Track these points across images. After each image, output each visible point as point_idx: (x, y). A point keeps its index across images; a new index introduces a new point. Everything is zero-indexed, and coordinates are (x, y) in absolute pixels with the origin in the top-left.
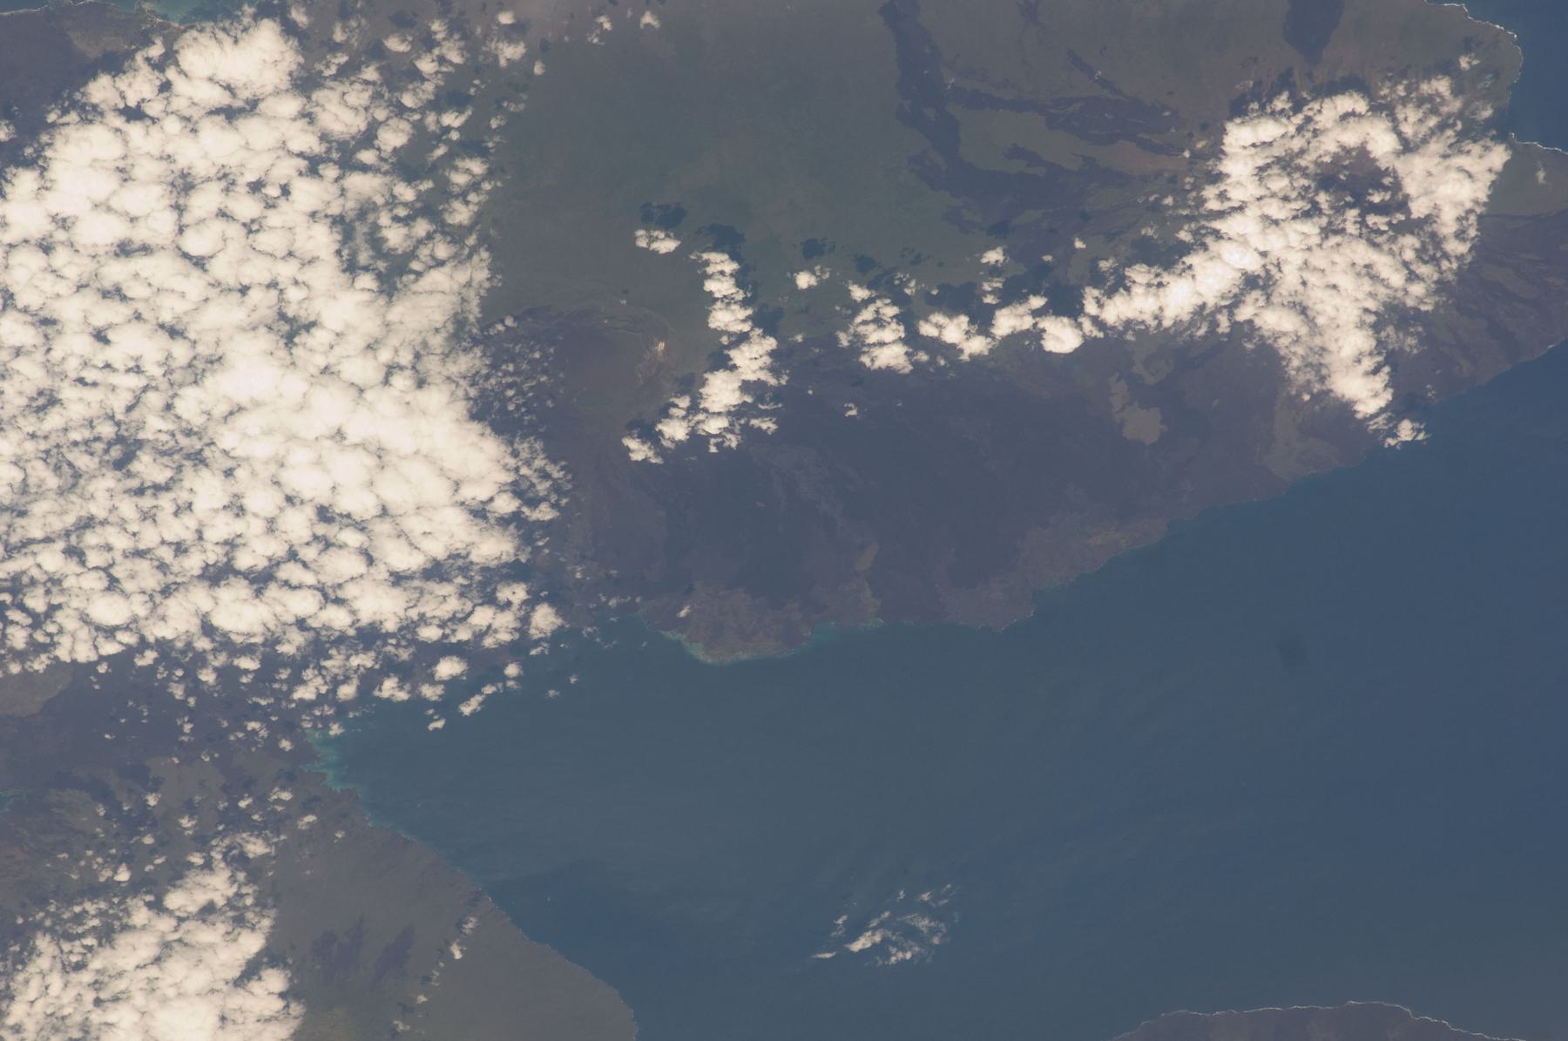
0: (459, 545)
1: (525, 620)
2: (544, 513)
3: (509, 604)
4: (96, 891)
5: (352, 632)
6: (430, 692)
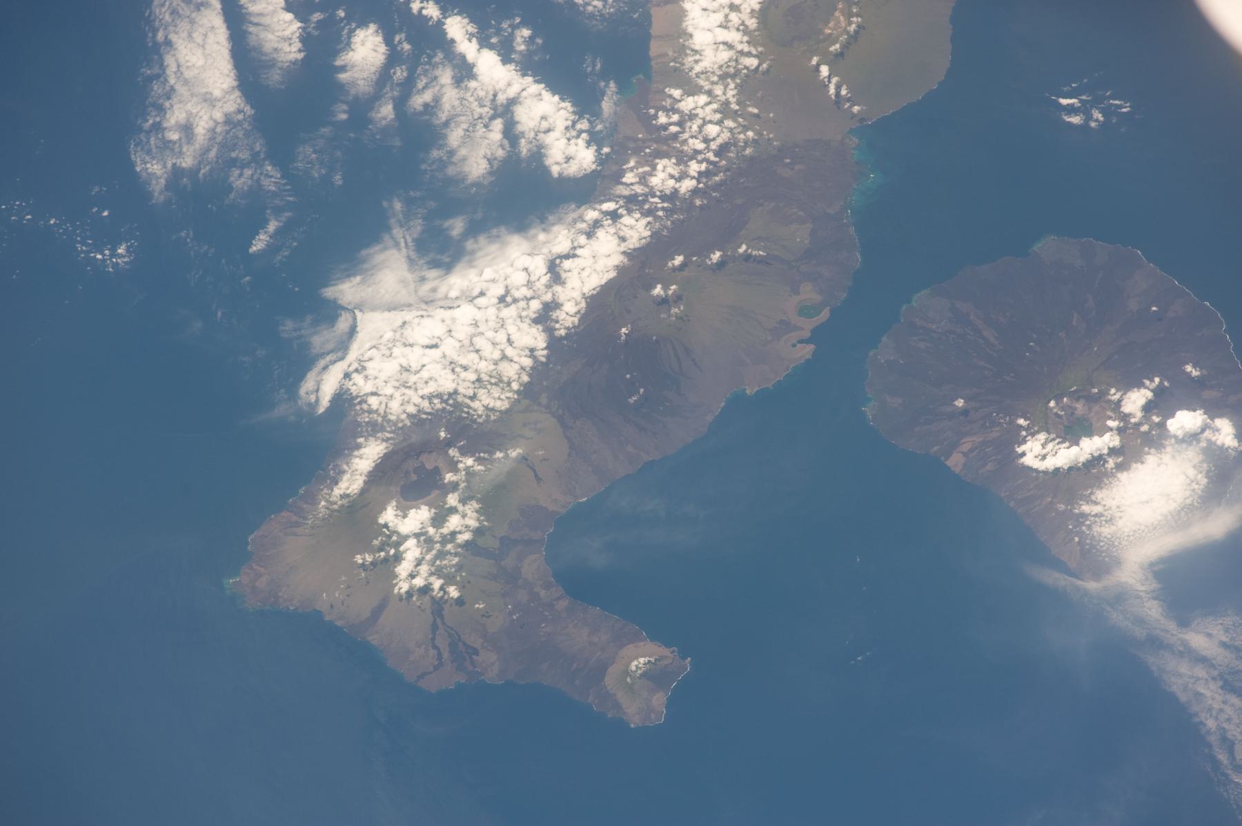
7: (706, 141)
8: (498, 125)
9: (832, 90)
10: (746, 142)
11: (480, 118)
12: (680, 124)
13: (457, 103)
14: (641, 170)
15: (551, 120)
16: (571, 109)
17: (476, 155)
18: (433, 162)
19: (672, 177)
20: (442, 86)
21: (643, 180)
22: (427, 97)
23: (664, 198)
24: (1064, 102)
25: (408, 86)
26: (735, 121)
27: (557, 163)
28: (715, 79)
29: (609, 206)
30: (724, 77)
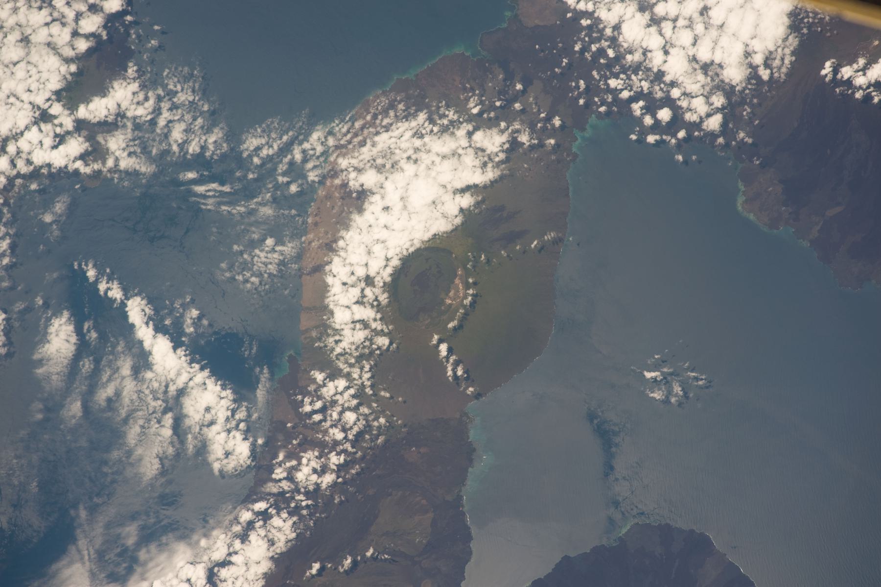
0: (727, 62)
1: (709, 115)
2: (765, 74)
3: (712, 104)
4: (462, 109)
5: (655, 70)
6: (648, 120)
7: (344, 430)
8: (168, 420)
9: (450, 373)
10: (379, 427)
11: (154, 412)
12: (323, 410)
13: (135, 397)
14: (288, 464)
15: (213, 412)
16: (231, 397)
17: (149, 449)
18: (114, 464)
19: (315, 471)
20: (123, 378)
21: (290, 478)
22: (110, 391)
23: (308, 494)
24: (649, 375)
25: (93, 382)
26: (369, 407)
27: (218, 459)
28: (353, 361)
29: (261, 506)
30: (360, 358)
